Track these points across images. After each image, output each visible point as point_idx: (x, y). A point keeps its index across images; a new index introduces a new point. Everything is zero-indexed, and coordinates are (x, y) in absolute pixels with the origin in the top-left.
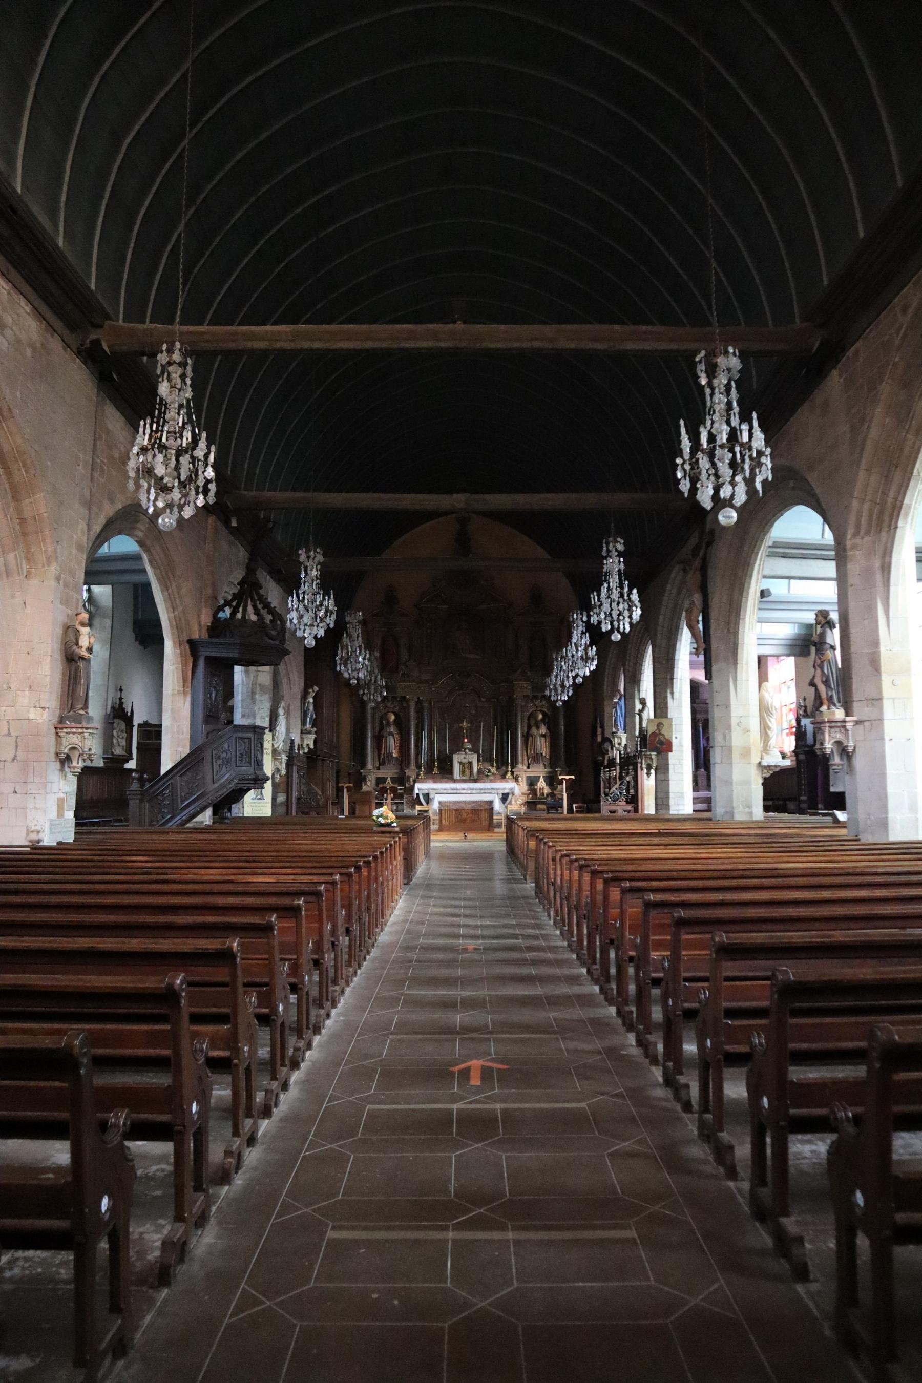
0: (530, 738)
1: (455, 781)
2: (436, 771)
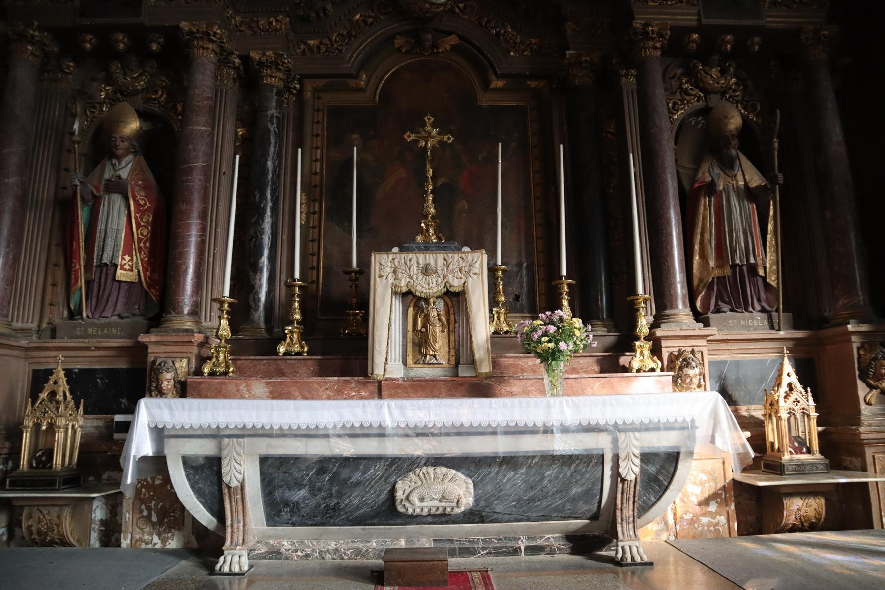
0: (704, 201)
1: (380, 390)
2: (292, 342)
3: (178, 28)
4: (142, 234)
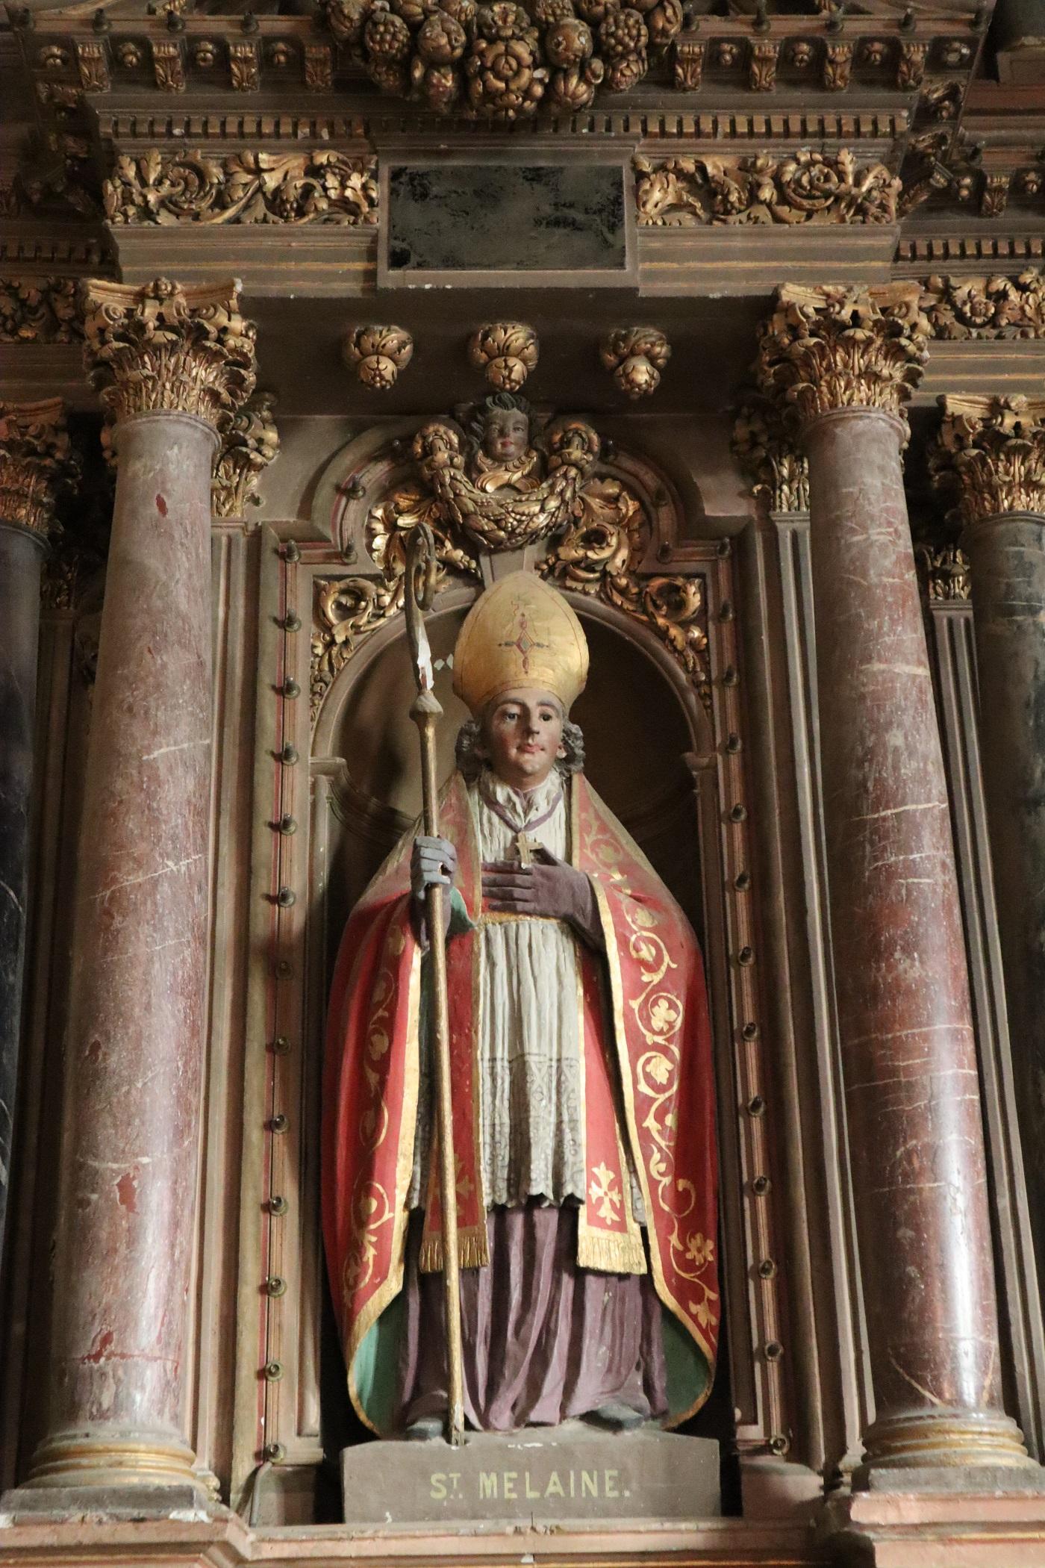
3: (769, 305)
4: (648, 1077)
